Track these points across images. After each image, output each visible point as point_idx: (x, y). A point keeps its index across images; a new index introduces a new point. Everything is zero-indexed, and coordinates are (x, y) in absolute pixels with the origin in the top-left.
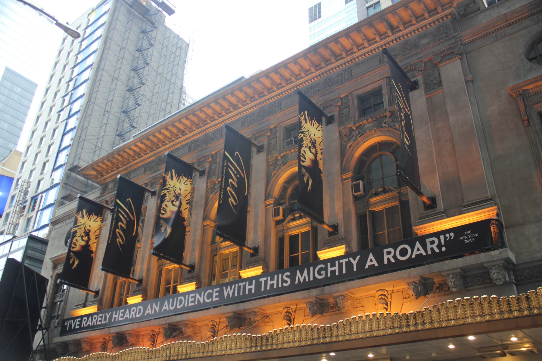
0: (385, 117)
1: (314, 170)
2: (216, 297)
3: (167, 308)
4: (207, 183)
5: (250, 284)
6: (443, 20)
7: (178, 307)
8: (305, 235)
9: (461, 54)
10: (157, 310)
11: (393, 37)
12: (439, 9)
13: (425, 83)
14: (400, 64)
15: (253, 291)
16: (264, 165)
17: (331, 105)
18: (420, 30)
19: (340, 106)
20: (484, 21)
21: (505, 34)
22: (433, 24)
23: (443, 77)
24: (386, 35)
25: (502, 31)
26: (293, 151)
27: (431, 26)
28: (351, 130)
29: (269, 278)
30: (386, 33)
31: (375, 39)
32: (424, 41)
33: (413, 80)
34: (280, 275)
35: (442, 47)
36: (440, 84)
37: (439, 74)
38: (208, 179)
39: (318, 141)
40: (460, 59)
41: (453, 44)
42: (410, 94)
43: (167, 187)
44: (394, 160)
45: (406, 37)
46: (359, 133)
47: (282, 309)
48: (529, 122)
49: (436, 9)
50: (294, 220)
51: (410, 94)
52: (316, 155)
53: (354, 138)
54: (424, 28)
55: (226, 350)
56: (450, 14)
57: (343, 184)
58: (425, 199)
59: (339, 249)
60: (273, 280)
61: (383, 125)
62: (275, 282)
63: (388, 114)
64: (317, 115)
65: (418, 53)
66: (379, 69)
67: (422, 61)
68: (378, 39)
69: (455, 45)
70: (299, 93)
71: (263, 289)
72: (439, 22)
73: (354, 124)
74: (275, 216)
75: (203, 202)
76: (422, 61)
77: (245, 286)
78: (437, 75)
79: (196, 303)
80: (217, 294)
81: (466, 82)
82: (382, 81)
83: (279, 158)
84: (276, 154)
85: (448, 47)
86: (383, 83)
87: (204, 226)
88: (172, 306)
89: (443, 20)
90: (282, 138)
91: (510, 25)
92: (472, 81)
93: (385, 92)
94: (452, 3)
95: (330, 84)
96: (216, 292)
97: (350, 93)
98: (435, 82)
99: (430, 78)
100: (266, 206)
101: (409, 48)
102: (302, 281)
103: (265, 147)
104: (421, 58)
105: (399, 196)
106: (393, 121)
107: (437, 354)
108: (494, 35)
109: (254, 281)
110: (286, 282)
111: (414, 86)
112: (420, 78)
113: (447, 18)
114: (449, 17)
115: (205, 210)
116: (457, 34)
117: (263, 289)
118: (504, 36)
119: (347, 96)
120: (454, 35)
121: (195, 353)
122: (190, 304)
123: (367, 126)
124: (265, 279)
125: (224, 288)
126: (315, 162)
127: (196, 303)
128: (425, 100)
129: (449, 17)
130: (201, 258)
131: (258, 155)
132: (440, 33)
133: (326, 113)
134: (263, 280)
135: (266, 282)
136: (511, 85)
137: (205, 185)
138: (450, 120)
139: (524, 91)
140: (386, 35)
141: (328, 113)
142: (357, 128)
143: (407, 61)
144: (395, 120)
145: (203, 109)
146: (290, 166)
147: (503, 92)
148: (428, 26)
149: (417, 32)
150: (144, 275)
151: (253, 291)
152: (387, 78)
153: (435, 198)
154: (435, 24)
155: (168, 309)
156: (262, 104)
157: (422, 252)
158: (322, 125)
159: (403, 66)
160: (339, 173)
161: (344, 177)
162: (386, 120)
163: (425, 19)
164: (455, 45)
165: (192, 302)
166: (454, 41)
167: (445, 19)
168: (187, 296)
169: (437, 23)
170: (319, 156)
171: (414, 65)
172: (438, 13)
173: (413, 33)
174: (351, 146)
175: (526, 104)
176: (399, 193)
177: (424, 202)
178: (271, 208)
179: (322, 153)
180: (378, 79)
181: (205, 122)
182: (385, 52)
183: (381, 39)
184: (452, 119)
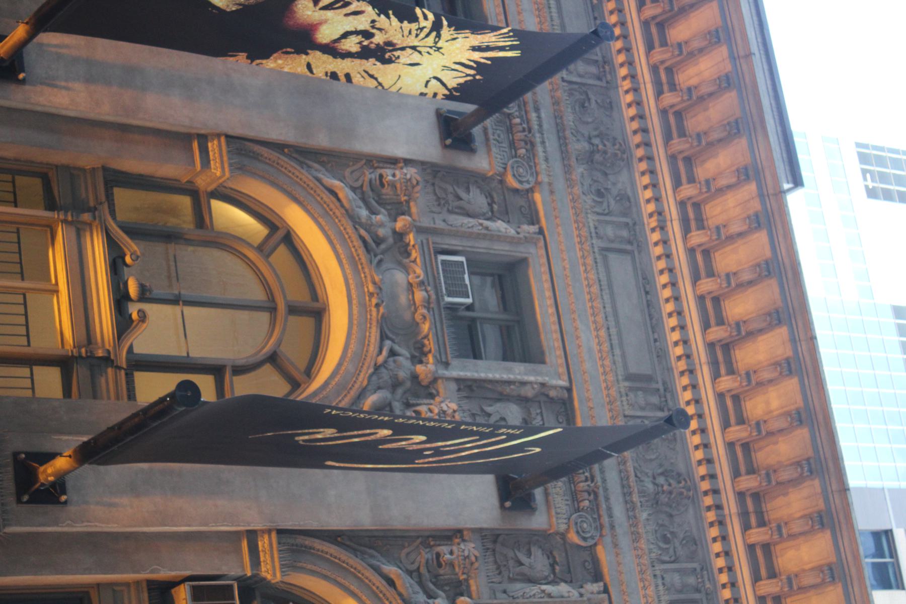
0: (419, 356)
1: (268, 29)
4: (407, 162)
16: (441, 520)
17: (512, 145)
19: (502, 182)
26: (420, 295)
28: (398, 209)
38: (423, 165)
39: (387, 74)
43: (446, 32)
46: (378, 241)
52: (331, 50)
53: (364, 213)
57: (235, 536)
58: (61, 463)
61: (388, 343)
64: (490, 92)
70: (598, 35)
73: (420, 230)
75: (322, 140)
82: (562, 370)
83: (401, 223)
84: (421, 208)
86: (550, 375)
90: (482, 246)
93: (518, 371)
95: (598, 157)
97: (541, 232)
101: (664, 498)
103: (463, 161)
105: (91, 357)
106: (395, 384)
111: (514, 491)
115: (279, 147)
119: (533, 219)
123: (400, 277)
126: (303, 40)
130: (50, 122)
131: (433, 118)
133: (488, 122)
137: (400, 151)
141: (485, 130)
142: (399, 236)
144: (400, 391)
145: (752, 187)
152: (569, 390)
153: (57, 502)
156: (623, 71)
158: (447, 97)
159: (602, 471)
160: (238, 131)
161: (212, 146)
170: (323, 64)
174: (335, 195)
176: (107, 360)
177: (50, 457)
178: (233, 566)
179: (334, 76)
181: (684, 166)
182: (676, 420)
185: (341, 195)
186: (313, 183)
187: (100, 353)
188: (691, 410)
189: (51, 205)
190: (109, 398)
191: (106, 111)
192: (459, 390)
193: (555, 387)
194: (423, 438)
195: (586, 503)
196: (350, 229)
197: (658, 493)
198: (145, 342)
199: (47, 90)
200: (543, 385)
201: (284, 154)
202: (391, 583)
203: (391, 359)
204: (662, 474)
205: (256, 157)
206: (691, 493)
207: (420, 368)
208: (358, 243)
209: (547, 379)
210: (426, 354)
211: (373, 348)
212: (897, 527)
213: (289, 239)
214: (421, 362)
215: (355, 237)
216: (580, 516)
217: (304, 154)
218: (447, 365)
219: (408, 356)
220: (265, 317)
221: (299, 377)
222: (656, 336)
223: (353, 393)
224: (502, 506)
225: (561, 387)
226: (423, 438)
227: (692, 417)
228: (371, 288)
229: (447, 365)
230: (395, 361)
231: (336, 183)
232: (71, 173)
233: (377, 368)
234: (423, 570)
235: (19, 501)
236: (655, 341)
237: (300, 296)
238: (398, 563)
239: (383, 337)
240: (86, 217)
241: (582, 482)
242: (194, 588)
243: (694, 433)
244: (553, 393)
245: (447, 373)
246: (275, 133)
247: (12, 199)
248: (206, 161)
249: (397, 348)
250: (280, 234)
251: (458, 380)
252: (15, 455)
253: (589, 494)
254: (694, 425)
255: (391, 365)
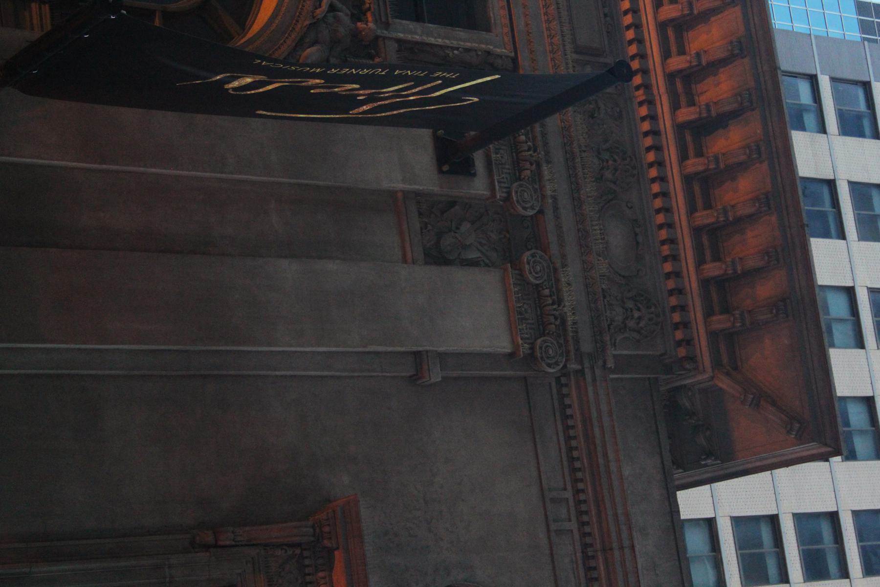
0: (359, 15)
6: (676, 326)
9: (531, 358)
11: (666, 124)
12: (720, 322)
13: (452, 204)
14: (553, 122)
18: (664, 234)
20: (626, 472)
21: (559, 532)
22: (671, 284)
23: (460, 274)
24: (683, 100)
25: (573, 525)
27: (668, 276)
30: (691, 103)
31: (682, 52)
32: (617, 237)
33: (478, 159)
35: (573, 297)
36: (437, 257)
37: (473, 263)
40: (511, 355)
41: (577, 341)
42: (425, 135)
44: (172, 7)
45: (653, 173)
48: (207, 547)
49: (726, 310)
51: (425, 135)
54: (666, 250)
56: (692, 358)
63: (369, 26)
65: (577, 203)
66: (557, 39)
67: (541, 212)
68: (677, 63)
69: (571, 347)
72: (674, 309)
76: (541, 212)
78: (473, 255)
81: (417, 355)
85: (570, 320)
86: (496, 42)
89: (676, 326)
91: (586, 558)
92: (415, 379)
93: (460, 39)
94: (728, 374)
98: (448, 241)
99: (466, 226)
101: (608, 175)
104: (556, 209)
108: (569, 494)
111: (452, 158)
112: (478, 187)
113: (679, 343)
114: (682, 352)
116: (610, 364)
118: (553, 527)
120: (611, 352)
128: (386, 185)
129: (682, 352)
132: (630, 304)
136: (364, 512)
138: (284, 263)
139: (330, 551)
140: (683, 100)
143: (558, 155)
147: (346, 479)
148: (668, 267)
149: (660, 218)
152: (515, 60)
154: (671, 292)
159: (544, 135)
162: (344, 16)
163: (700, 262)
164: (571, 347)
166: (587, 347)
167: (679, 335)
169: (673, 301)
171: (538, 176)
172: (709, 313)
173: (658, 203)
175: (279, 552)
180: (520, 24)
182: (620, 72)
183: (671, 77)
184: (288, 270)
188: (635, 65)
190: (32, 29)
192: (399, 51)
193: (500, 56)
194: (358, 86)
195: (528, 172)
197: (603, 168)
200: (488, 53)
203: (332, 14)
204: (607, 150)
206: (635, 172)
207: (360, 25)
209: (491, 47)
210: (365, 14)
212: (822, 74)
214: (360, 20)
216: (521, 186)
218: (387, 26)
219: (349, 13)
222: (607, 10)
224: (440, 171)
225: (507, 57)
226: (358, 86)
227: (636, 72)
229: (387, 26)
230: (335, 17)
236: (606, 15)
241: (525, 151)
243: (638, 88)
244: (499, 62)
245: (386, 33)
251: (399, 41)
253: (531, 164)
254: (638, 80)
255: (330, 19)
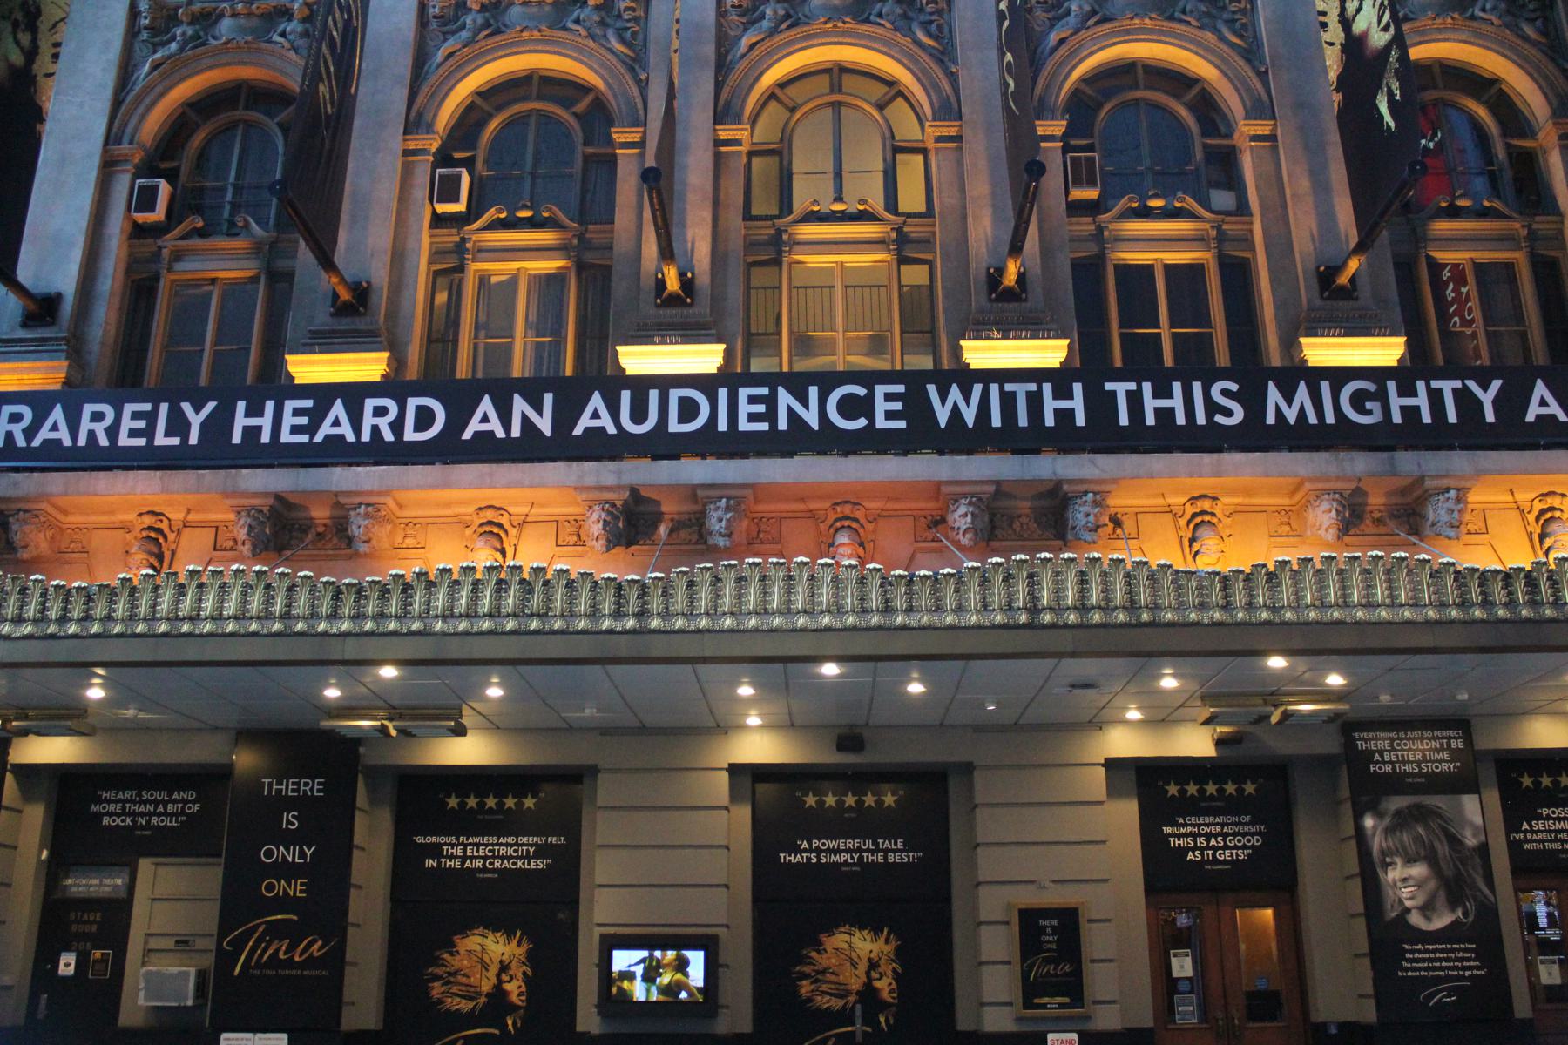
2: (890, 415)
3: (606, 422)
5: (1063, 392)
7: (674, 427)
8: (1185, 279)
10: (545, 424)
15: (1080, 421)
29: (1147, 387)
34: (1197, 387)
47: (132, 516)
50: (1145, 213)
55: (221, 617)
59: (1383, 345)
60: (260, 413)
62: (266, 422)
71: (1124, 420)
74: (1078, 183)
75: (710, 50)
77: (1035, 401)
79: (783, 425)
80: (898, 406)
87: (718, 143)
88: (639, 415)
96: (889, 397)
100: (406, 153)
102: (1292, 421)
107: (998, 704)
109: (1078, 388)
110: (1228, 413)
115: (719, 86)
117: (1124, 420)
121: (1202, 606)
122: (744, 425)
124: (1132, 386)
125: (932, 389)
127: (783, 425)
134: (1121, 389)
135: (1135, 400)
146: (1128, 32)
150: (379, 275)
151: (1080, 421)
155: (611, 430)
157: (495, 426)
165: (753, 418)
168: (723, 393)
185: (754, 40)
186: (745, 61)
187: (894, 235)
189: (777, 262)
191: (707, 215)
196: (782, 36)
198: (877, 203)
199: (696, 256)
201: (724, 81)
202: (1062, 41)
205: (728, 103)
208: (792, 32)
211: (879, 30)
213: (783, 85)
215: (787, 34)
217: (722, 67)
220: (844, 110)
221: (893, 92)
223: (917, 50)
228: (830, 25)
231: (745, 42)
232: (751, 245)
233: (895, 29)
234: (1050, 15)
235: (1025, 300)
237: (824, 81)
238: (1046, 34)
239: (867, 21)
240: (785, 237)
242: (1074, 184)
246: (709, 87)
247: (826, 291)
248: (737, 142)
249: (876, 11)
250: (777, 91)
252: (990, 300)
